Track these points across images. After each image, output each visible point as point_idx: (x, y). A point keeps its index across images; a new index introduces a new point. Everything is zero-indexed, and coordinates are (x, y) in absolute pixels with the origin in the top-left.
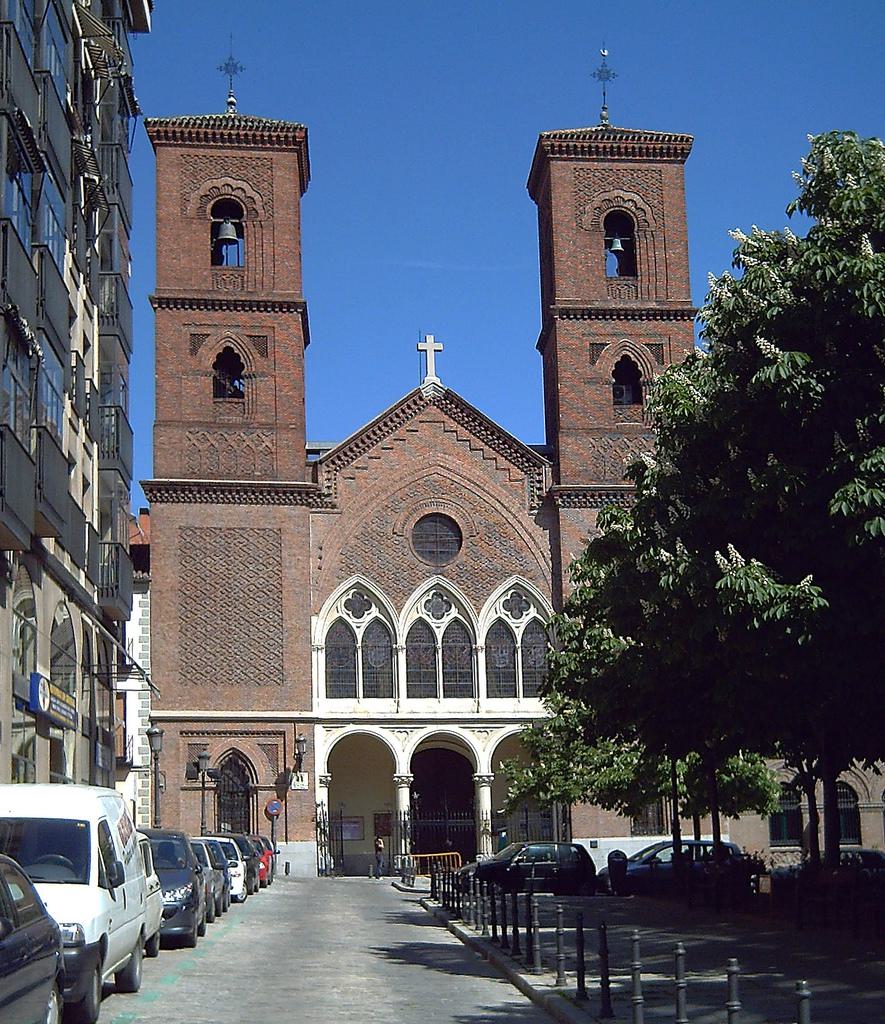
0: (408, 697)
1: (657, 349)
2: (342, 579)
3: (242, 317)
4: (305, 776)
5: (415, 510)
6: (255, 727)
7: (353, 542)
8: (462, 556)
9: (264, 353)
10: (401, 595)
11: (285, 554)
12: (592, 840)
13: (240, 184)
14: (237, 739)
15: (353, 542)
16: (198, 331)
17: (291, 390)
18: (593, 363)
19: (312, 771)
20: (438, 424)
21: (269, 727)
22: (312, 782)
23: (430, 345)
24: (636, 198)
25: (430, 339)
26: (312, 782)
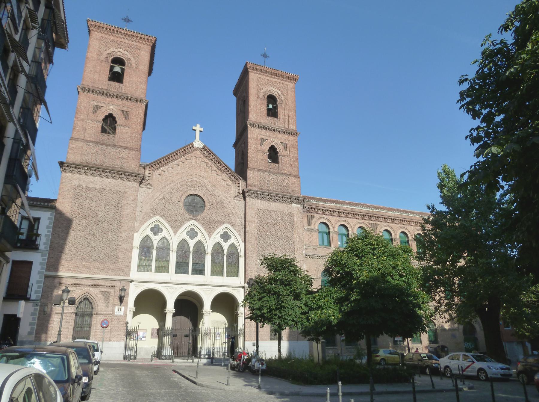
0: (176, 273)
1: (285, 145)
2: (151, 217)
3: (119, 102)
6: (100, 283)
7: (157, 201)
8: (205, 213)
9: (127, 118)
10: (176, 227)
11: (125, 203)
13: (126, 52)
14: (90, 289)
16: (99, 104)
17: (136, 135)
18: (261, 145)
19: (126, 306)
20: (199, 159)
21: (107, 283)
22: (126, 312)
23: (198, 128)
24: (279, 92)
25: (198, 126)
26: (126, 312)
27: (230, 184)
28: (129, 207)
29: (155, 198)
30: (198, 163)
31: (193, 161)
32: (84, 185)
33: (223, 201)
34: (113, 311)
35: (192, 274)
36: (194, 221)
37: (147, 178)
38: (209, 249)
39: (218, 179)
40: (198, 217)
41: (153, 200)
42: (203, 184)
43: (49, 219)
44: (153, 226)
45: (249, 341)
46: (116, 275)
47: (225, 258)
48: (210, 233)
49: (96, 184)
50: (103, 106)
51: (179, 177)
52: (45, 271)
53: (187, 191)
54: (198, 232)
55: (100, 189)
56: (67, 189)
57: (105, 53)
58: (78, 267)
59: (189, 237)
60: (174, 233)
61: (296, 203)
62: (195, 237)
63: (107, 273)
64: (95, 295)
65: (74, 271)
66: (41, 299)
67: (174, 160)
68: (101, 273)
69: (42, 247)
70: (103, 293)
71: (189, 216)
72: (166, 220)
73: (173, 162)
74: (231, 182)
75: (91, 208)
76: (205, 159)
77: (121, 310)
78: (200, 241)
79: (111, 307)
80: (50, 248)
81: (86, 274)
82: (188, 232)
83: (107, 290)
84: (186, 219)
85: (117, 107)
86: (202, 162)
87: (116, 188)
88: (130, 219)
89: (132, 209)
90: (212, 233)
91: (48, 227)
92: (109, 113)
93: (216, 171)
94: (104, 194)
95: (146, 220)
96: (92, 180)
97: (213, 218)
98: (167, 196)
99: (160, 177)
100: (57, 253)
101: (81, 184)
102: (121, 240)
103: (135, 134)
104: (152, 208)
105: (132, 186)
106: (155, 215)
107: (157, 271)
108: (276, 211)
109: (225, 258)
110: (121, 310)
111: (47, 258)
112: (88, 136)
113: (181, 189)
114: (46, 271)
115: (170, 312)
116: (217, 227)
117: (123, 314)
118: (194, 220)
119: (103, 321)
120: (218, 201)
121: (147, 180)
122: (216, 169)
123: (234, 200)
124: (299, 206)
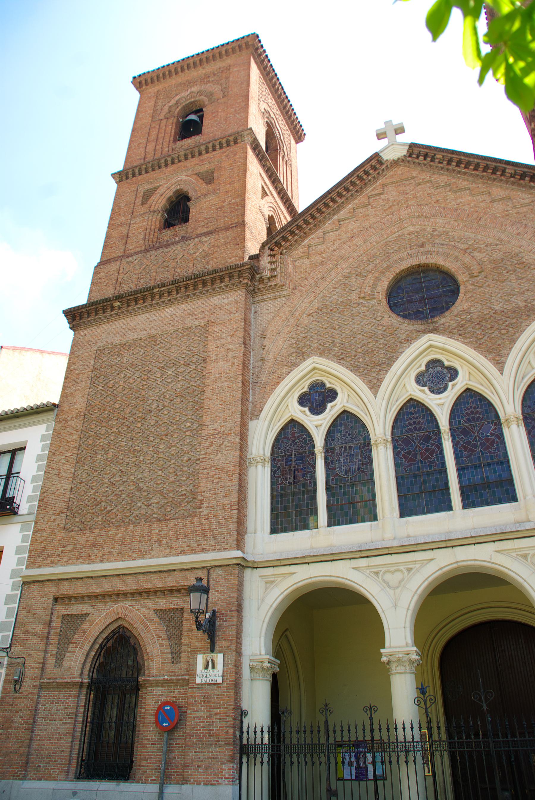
4: (219, 658)
5: (388, 268)
7: (306, 321)
11: (211, 347)
14: (127, 604)
15: (306, 321)
20: (408, 182)
27: (527, 201)
28: (222, 354)
29: (297, 313)
30: (408, 191)
31: (392, 193)
32: (117, 340)
33: (517, 250)
34: (191, 672)
35: (466, 506)
36: (429, 334)
37: (266, 274)
39: (482, 204)
40: (442, 321)
41: (292, 321)
42: (436, 233)
43: (43, 438)
44: (306, 389)
46: (194, 551)
49: (142, 330)
50: (161, 184)
51: (358, 241)
52: (24, 567)
53: (388, 268)
54: (456, 364)
55: (152, 337)
56: (81, 363)
58: (96, 545)
59: (426, 389)
60: (371, 389)
62: (450, 384)
63: (168, 551)
64: (143, 622)
65: (89, 559)
66: (11, 646)
68: (153, 553)
69: (24, 508)
70: (162, 613)
71: (411, 327)
72: (340, 359)
73: (336, 217)
74: (525, 196)
75: (132, 386)
76: (425, 176)
77: (213, 667)
78: (468, 389)
79: (184, 657)
80: (39, 506)
81: (116, 560)
83: (175, 602)
84: (403, 337)
85: (189, 173)
86: (419, 184)
87: (188, 322)
88: (226, 384)
89: (229, 357)
90: (503, 352)
91: (39, 458)
92: (174, 190)
93: (465, 189)
94: (160, 346)
95: (281, 378)
96: (132, 324)
97: (498, 308)
98: (333, 297)
99: (307, 262)
100: (53, 517)
101: (109, 341)
102: (206, 444)
103: (229, 199)
104: (293, 341)
105: (226, 301)
106: (303, 356)
107: (333, 521)
110: (213, 667)
111: (31, 533)
112: (130, 248)
114: (26, 568)
115: (399, 659)
117: (220, 680)
118: (431, 331)
119: (160, 708)
120: (498, 255)
121: (269, 279)
122: (465, 183)
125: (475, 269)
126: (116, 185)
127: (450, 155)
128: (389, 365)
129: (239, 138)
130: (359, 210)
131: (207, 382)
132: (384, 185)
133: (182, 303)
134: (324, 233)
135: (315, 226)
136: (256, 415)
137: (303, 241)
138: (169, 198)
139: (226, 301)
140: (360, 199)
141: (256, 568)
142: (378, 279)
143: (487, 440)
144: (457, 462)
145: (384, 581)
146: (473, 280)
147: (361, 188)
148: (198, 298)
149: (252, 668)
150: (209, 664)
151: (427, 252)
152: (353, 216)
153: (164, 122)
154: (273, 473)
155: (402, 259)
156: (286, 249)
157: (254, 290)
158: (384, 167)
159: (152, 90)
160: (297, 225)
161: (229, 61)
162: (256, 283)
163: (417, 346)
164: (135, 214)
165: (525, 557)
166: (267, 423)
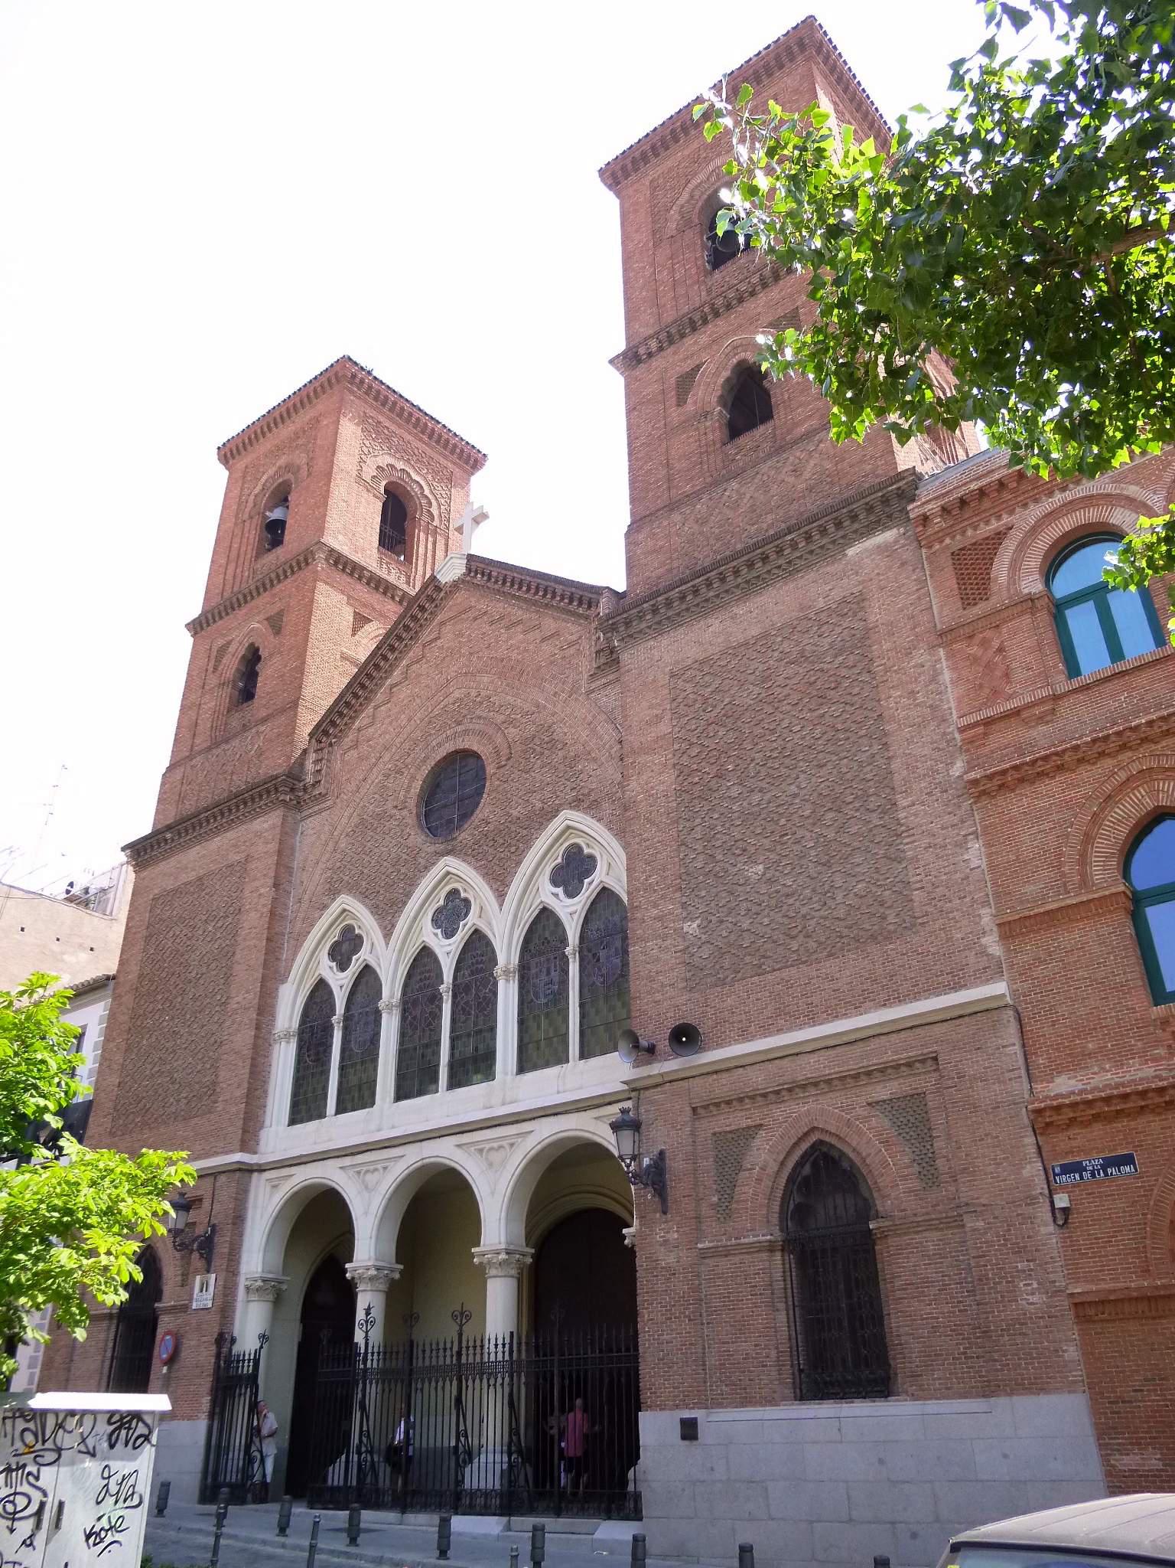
5: (424, 761)
8: (485, 810)
12: (687, 1414)
18: (681, 401)
27: (574, 638)
37: (309, 779)
38: (507, 953)
41: (330, 848)
45: (662, 1408)
47: (574, 969)
48: (500, 883)
53: (427, 758)
57: (252, 497)
61: (870, 530)
67: (389, 673)
71: (431, 849)
73: (389, 682)
82: (439, 911)
86: (475, 619)
106: (333, 893)
108: (765, 635)
109: (574, 969)
113: (409, 760)
116: (528, 843)
118: (448, 853)
121: (313, 785)
122: (520, 612)
123: (593, 691)
124: (888, 536)
125: (505, 752)
126: (192, 640)
127: (504, 572)
128: (405, 903)
129: (309, 556)
130: (414, 667)
131: (239, 939)
132: (442, 623)
133: (226, 831)
134: (376, 708)
135: (366, 698)
136: (284, 979)
137: (353, 723)
138: (243, 657)
139: (266, 825)
140: (415, 651)
141: (265, 1170)
142: (413, 778)
143: (485, 998)
144: (453, 1030)
145: (363, 1181)
146: (502, 770)
147: (416, 632)
148: (243, 823)
149: (248, 1288)
150: (204, 1286)
151: (466, 732)
152: (406, 678)
153: (247, 524)
154: (300, 1048)
155: (439, 745)
156: (335, 737)
157: (298, 803)
158: (442, 594)
159: (241, 464)
160: (345, 702)
161: (321, 406)
162: (300, 794)
163: (433, 875)
164: (207, 687)
165: (481, 1151)
166: (295, 986)
